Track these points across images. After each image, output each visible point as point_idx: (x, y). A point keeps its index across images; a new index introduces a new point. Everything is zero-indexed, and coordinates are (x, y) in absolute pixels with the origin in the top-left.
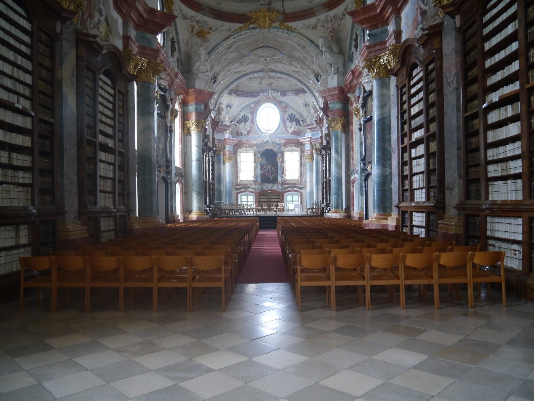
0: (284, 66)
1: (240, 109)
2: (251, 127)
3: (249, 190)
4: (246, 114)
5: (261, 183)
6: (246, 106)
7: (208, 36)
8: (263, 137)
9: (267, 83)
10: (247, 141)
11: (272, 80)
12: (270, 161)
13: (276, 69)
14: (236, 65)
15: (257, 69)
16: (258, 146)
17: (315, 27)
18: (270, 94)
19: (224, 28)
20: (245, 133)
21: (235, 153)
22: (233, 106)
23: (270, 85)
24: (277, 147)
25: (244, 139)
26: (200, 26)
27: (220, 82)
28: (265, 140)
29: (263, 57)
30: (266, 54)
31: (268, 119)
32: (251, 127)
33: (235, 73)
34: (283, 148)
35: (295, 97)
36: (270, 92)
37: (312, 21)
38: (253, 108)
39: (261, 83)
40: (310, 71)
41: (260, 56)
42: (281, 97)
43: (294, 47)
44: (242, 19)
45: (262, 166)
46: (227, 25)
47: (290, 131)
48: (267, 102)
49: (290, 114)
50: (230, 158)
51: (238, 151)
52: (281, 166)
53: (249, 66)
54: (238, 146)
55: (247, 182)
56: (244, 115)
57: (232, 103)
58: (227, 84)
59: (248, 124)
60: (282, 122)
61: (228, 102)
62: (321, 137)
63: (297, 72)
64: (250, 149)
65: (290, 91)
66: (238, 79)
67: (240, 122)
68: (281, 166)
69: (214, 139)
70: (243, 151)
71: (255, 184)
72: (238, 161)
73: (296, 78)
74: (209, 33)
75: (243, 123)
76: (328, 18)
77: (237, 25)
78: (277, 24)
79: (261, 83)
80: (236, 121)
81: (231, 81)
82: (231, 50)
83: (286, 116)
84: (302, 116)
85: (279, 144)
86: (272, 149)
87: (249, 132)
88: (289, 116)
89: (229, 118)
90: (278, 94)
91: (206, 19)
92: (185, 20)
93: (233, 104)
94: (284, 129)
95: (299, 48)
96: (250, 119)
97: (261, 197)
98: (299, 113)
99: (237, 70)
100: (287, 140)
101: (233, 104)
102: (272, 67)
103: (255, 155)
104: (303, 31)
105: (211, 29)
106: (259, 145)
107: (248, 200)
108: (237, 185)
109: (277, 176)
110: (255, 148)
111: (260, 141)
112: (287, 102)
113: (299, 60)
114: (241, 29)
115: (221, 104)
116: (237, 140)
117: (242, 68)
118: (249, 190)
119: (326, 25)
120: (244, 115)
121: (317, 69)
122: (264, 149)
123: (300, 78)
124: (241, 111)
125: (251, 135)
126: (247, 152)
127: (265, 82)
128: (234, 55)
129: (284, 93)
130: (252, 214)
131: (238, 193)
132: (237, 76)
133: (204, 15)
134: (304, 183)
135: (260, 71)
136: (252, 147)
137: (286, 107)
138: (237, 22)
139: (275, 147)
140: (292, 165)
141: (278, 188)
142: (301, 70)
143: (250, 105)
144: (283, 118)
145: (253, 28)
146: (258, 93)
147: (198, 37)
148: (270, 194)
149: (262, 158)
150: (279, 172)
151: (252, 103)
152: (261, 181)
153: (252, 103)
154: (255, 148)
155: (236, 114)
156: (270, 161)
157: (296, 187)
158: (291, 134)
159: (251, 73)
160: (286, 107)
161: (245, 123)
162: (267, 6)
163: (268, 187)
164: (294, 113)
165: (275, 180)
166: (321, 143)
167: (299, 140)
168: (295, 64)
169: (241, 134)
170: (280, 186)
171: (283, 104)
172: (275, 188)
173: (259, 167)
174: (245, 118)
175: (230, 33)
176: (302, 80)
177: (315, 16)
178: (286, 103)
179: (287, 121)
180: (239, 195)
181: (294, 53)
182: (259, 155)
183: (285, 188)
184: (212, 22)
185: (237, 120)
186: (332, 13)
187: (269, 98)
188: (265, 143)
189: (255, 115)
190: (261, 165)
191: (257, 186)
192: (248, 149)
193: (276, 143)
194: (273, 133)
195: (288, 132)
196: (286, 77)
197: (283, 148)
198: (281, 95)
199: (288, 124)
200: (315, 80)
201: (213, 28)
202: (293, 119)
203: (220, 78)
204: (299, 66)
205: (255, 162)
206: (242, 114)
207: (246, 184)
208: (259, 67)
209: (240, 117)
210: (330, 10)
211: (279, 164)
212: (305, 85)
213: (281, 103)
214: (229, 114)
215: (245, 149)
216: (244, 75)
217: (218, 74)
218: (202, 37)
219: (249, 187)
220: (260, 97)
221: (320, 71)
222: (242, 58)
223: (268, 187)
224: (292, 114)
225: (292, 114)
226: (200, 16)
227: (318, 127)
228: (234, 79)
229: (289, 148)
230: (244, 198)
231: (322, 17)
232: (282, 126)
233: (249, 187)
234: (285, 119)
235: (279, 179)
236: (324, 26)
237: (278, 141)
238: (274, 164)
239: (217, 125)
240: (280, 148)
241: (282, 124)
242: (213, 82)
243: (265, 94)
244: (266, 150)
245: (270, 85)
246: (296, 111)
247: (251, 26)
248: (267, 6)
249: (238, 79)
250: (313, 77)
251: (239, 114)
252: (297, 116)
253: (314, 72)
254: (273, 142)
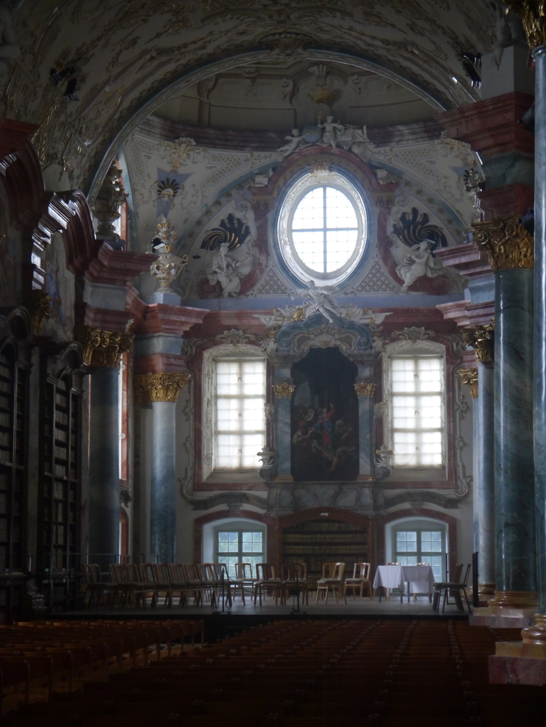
1: (212, 192)
2: (256, 265)
3: (246, 507)
4: (238, 215)
5: (290, 478)
6: (239, 184)
8: (299, 301)
10: (240, 316)
12: (327, 393)
13: (325, 37)
15: (248, 38)
16: (281, 334)
18: (328, 135)
20: (231, 285)
22: (187, 184)
23: (331, 99)
24: (357, 338)
25: (227, 309)
27: (96, 91)
28: (309, 313)
31: (324, 229)
32: (256, 265)
33: (161, 52)
34: (378, 343)
35: (425, 145)
36: (329, 127)
38: (264, 190)
39: (293, 94)
42: (371, 146)
45: (296, 413)
47: (408, 276)
48: (320, 165)
49: (408, 209)
50: (172, 383)
51: (206, 355)
52: (371, 412)
54: (204, 340)
55: (238, 477)
56: (231, 217)
57: (182, 170)
58: (135, 94)
59: (245, 251)
60: (375, 241)
61: (168, 168)
64: (251, 348)
65: (405, 123)
67: (212, 243)
68: (371, 412)
69: (80, 307)
70: (229, 358)
71: (269, 486)
72: (206, 396)
73: (402, 71)
75: (223, 249)
79: (293, 94)
80: (198, 242)
81: (148, 84)
83: (393, 220)
84: (454, 218)
85: (365, 330)
86: (336, 349)
87: (247, 283)
88: (403, 218)
89: (171, 227)
90: (361, 135)
93: (187, 176)
94: (385, 270)
96: (253, 231)
97: (292, 538)
98: (444, 209)
99: (165, 42)
100: (396, 312)
101: (187, 176)
102: (306, 29)
103: (271, 373)
106: (285, 334)
107: (239, 552)
108: (200, 486)
109: (357, 452)
110: (272, 345)
111: (290, 314)
112: (397, 164)
115: (114, 172)
116: (198, 314)
118: (246, 507)
120: (231, 217)
122: (306, 348)
123: (416, 70)
124: (218, 203)
125: (255, 295)
126: (241, 359)
129: (382, 134)
130: (246, 605)
131: (200, 522)
132: (171, 67)
136: (257, 337)
137: (391, 187)
139: (347, 340)
140: (417, 410)
141: (358, 499)
143: (251, 177)
144: (382, 227)
148: (325, 526)
149: (296, 381)
150: (365, 436)
151: (262, 172)
152: (294, 471)
153: (262, 172)
154: (272, 345)
155: (197, 213)
156: (327, 393)
158: (413, 288)
160: (391, 187)
161: (231, 248)
163: (319, 495)
164: (423, 209)
167: (439, 313)
169: (218, 289)
170: (367, 491)
171: (381, 174)
172: (347, 500)
173: (285, 417)
174: (232, 230)
176: (427, 77)
178: (392, 171)
179: (394, 238)
180: (208, 528)
182: (286, 373)
183: (390, 502)
185: (202, 236)
187: (323, 152)
188: (308, 325)
189: (270, 216)
191: (275, 492)
192: (243, 347)
193: (352, 326)
194: (342, 286)
195: (401, 282)
196: (364, 67)
197: (378, 343)
198: (372, 138)
199: (400, 250)
200: (463, 73)
202: (415, 230)
203: (94, 71)
205: (271, 397)
206: (222, 214)
207: (235, 485)
208: (257, 32)
209: (214, 223)
211: (364, 407)
212: (437, 95)
213: (371, 168)
214: (172, 214)
215: (230, 348)
216: (203, 63)
219: (245, 498)
220: (289, 148)
223: (319, 495)
224: (415, 211)
225: (415, 211)
228: (159, 75)
229: (405, 344)
230: (228, 543)
232: (376, 256)
233: (245, 498)
234: (390, 229)
235: (365, 467)
237: (358, 316)
239: (94, 254)
240: (368, 345)
241: (375, 252)
242: (63, 86)
243: (310, 136)
244: (315, 352)
245: (331, 99)
246: (431, 201)
251: (208, 212)
252: (434, 221)
253: (456, 42)
254: (340, 321)
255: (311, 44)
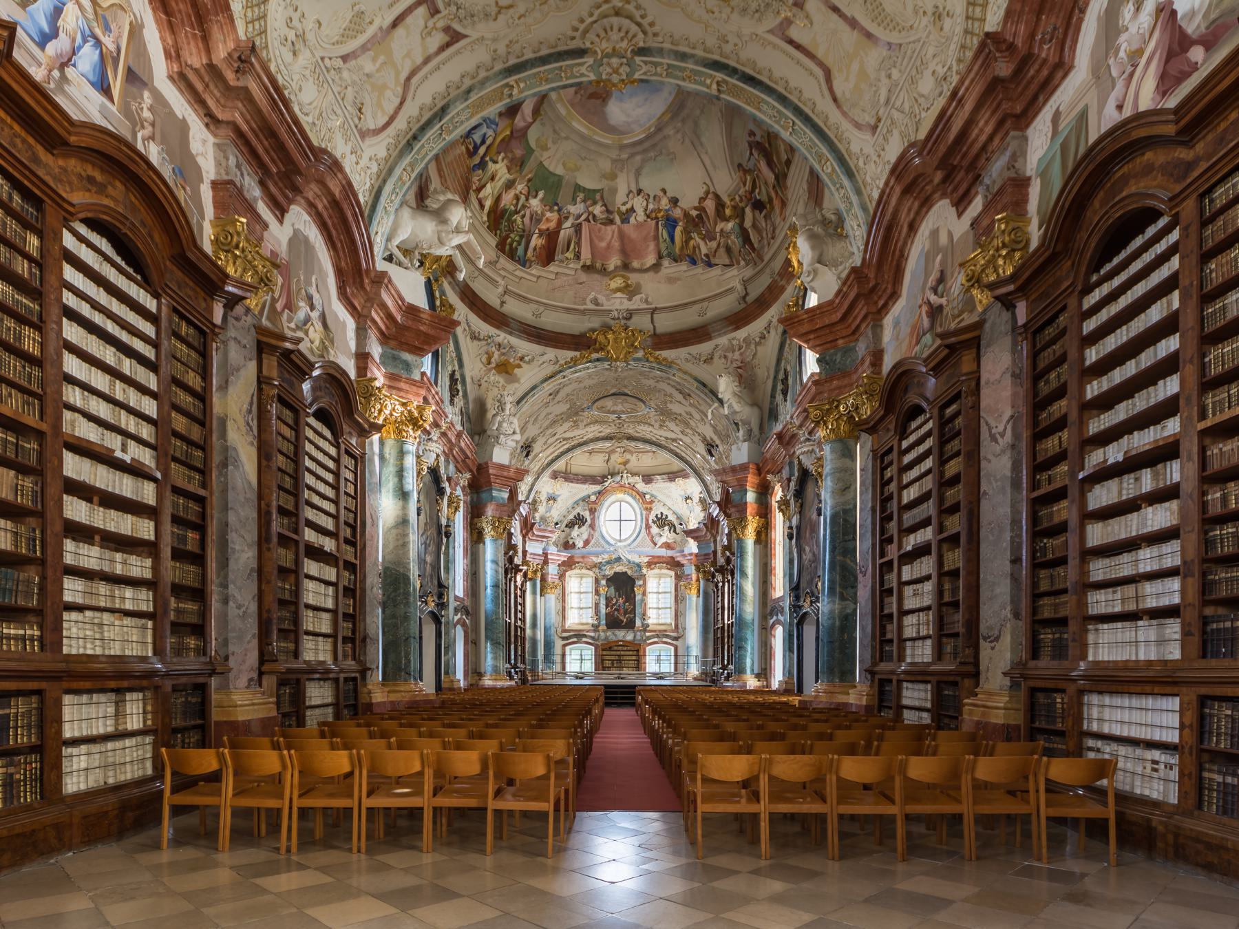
0: (651, 429)
7: (517, 371)
9: (620, 460)
11: (628, 456)
14: (567, 425)
17: (709, 360)
19: (545, 358)
21: (562, 577)
23: (625, 463)
26: (503, 354)
27: (536, 456)
29: (614, 412)
30: (619, 408)
37: (705, 348)
40: (697, 439)
41: (609, 412)
43: (671, 395)
44: (580, 343)
45: (608, 600)
46: (551, 353)
52: (643, 600)
53: (588, 429)
54: (569, 564)
55: (581, 627)
62: (715, 552)
63: (674, 440)
66: (568, 450)
69: (525, 552)
73: (671, 451)
74: (519, 366)
76: (734, 342)
77: (570, 354)
78: (640, 354)
82: (559, 398)
91: (514, 341)
92: (476, 342)
95: (680, 397)
104: (689, 367)
105: (522, 359)
108: (564, 631)
113: (674, 417)
114: (575, 362)
117: (577, 432)
119: (730, 355)
121: (709, 433)
127: (617, 458)
128: (564, 407)
129: (648, 479)
133: (511, 334)
134: (680, 630)
135: (608, 438)
138: (569, 349)
140: (658, 598)
142: (681, 436)
145: (598, 360)
146: (603, 478)
147: (499, 372)
150: (638, 610)
152: (607, 625)
156: (622, 588)
157: (667, 636)
159: (592, 441)
162: (623, 322)
165: (630, 625)
166: (714, 563)
168: (671, 425)
175: (557, 367)
177: (710, 339)
181: (670, 406)
182: (603, 582)
184: (524, 346)
186: (742, 334)
190: (607, 598)
200: (705, 454)
201: (527, 359)
203: (537, 447)
204: (677, 429)
208: (607, 431)
210: (737, 328)
211: (638, 598)
212: (687, 462)
216: (580, 445)
217: (534, 440)
218: (507, 373)
221: (715, 438)
222: (576, 414)
226: (502, 337)
227: (709, 536)
231: (723, 341)
235: (638, 623)
236: (725, 357)
238: (630, 598)
245: (625, 463)
247: (595, 356)
248: (623, 322)
249: (568, 450)
250: (701, 448)
253: (704, 439)
255: (631, 438)
